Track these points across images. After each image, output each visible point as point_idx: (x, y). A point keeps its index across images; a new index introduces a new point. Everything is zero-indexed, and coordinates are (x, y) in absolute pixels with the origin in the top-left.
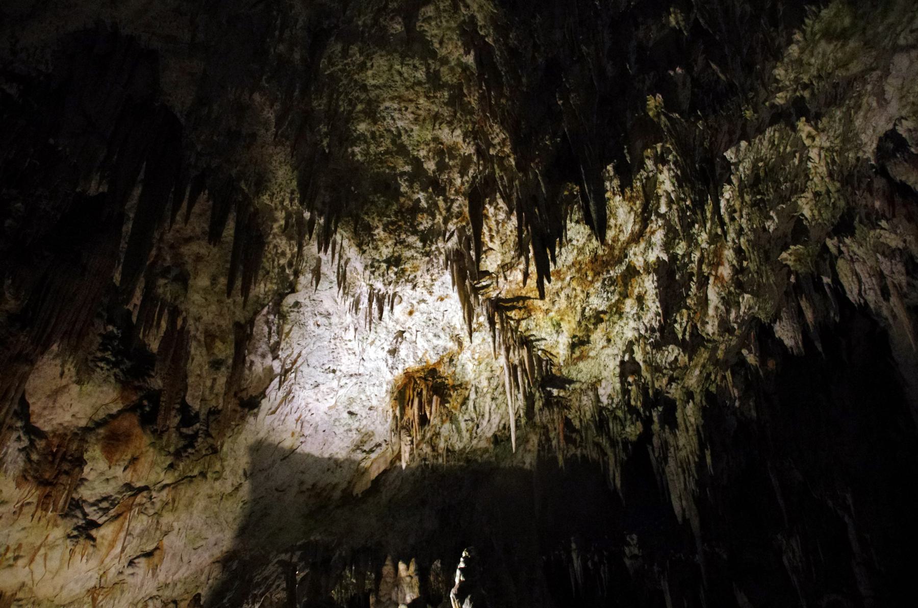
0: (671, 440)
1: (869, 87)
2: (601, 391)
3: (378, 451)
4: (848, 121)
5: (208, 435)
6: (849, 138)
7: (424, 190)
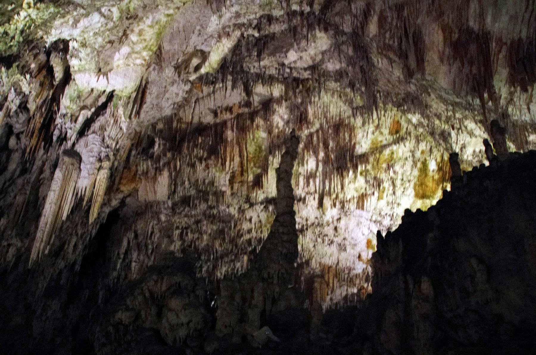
1: (75, 13)
4: (53, 17)
6: (46, 24)
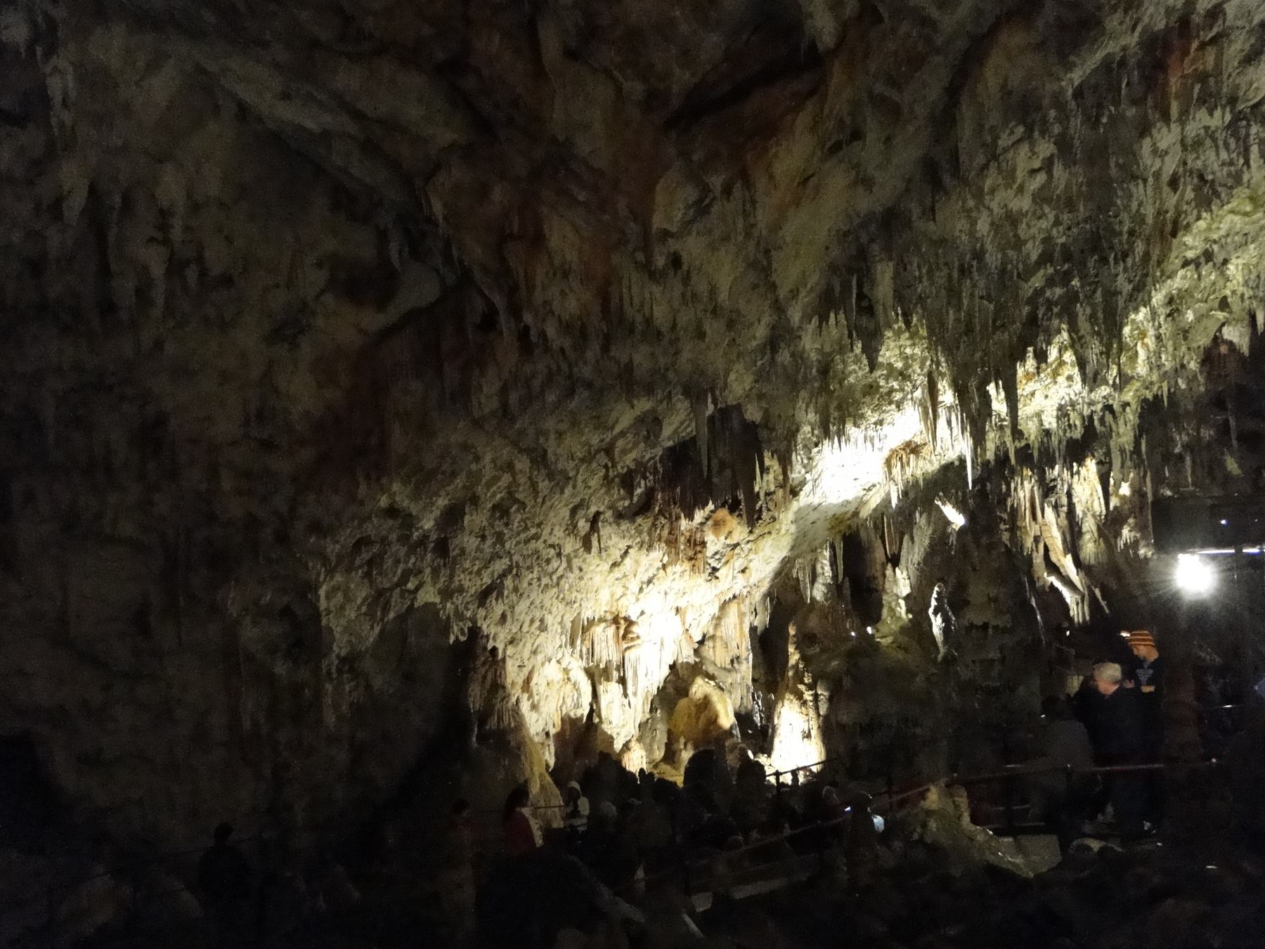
0: (1114, 427)
2: (1043, 417)
3: (874, 490)
5: (769, 510)
7: (896, 380)
